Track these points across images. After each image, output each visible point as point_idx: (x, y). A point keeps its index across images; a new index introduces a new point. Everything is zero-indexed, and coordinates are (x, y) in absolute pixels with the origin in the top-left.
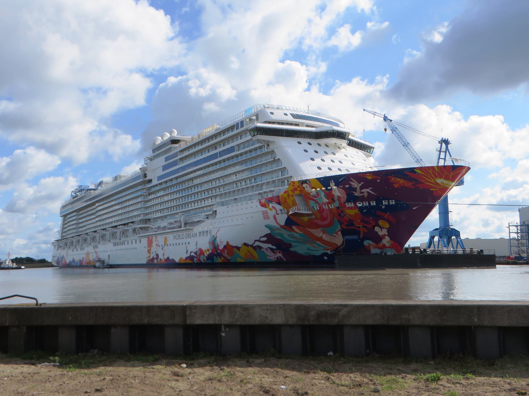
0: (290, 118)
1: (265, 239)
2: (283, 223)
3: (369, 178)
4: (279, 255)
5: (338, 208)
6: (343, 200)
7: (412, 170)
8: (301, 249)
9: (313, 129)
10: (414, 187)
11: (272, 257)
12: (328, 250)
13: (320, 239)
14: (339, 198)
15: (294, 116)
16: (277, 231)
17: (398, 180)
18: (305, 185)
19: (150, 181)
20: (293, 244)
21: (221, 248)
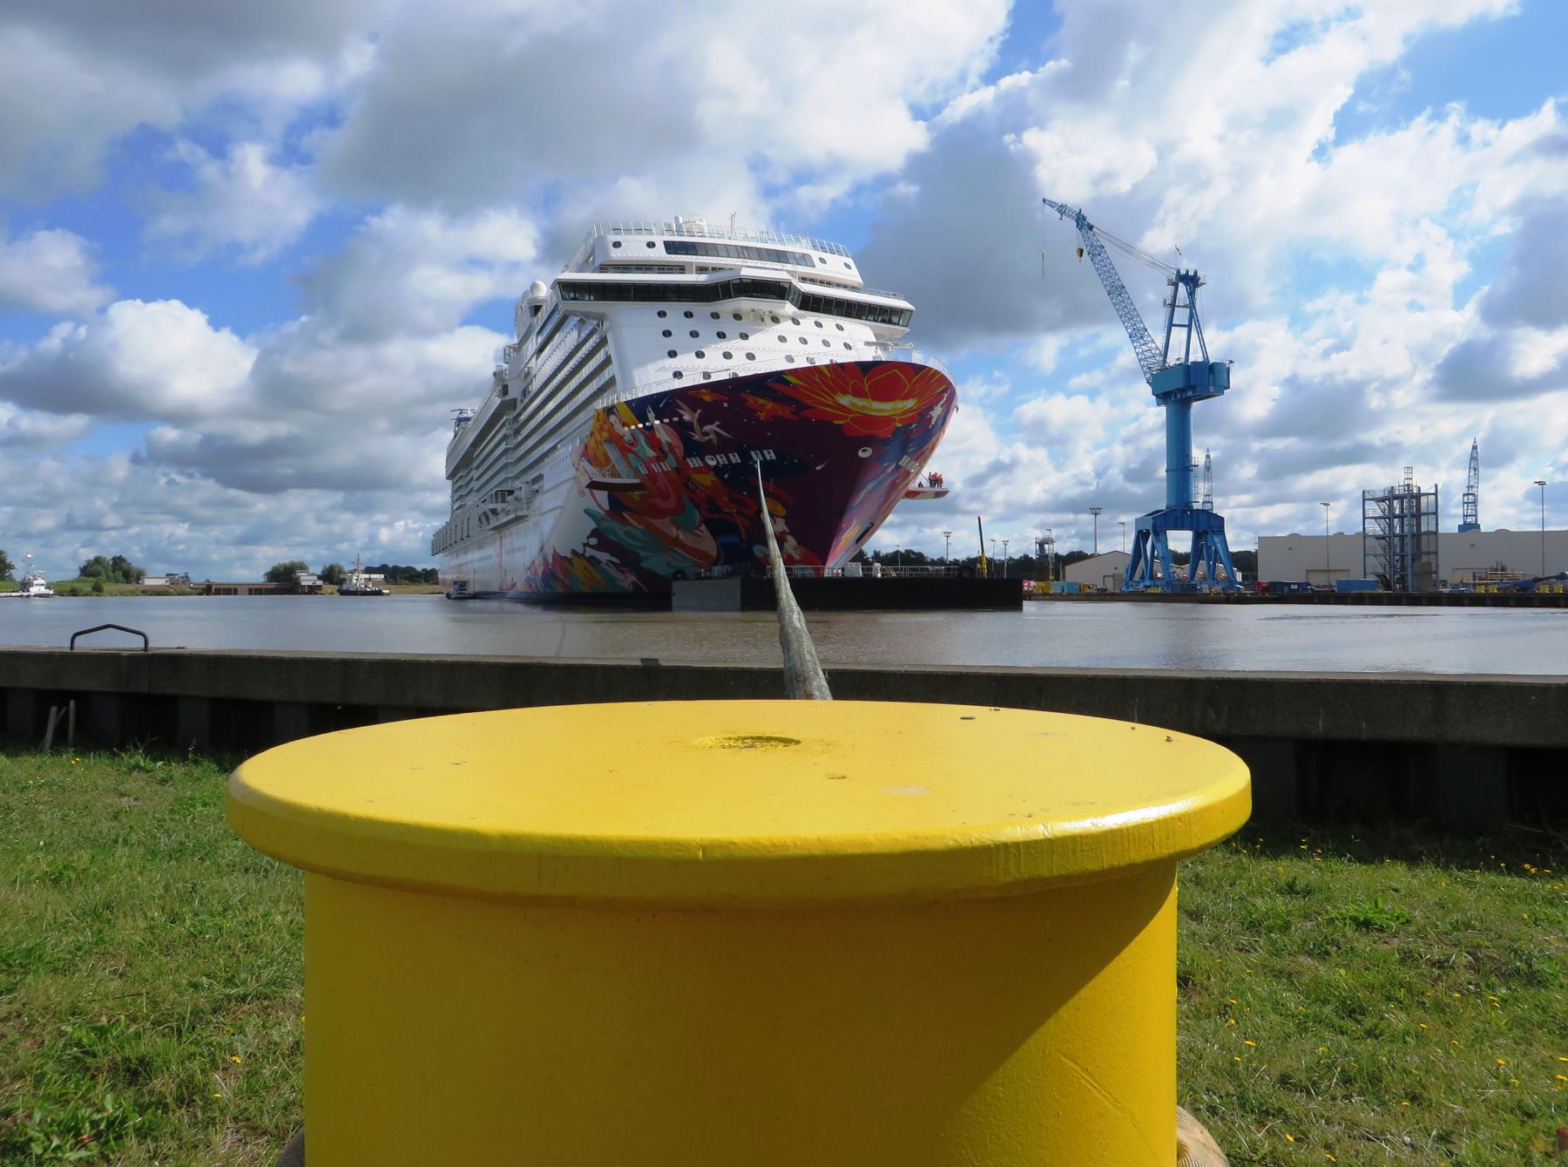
0: (659, 254)
3: (708, 398)
4: (632, 578)
5: (677, 470)
6: (680, 451)
7: (778, 376)
8: (658, 563)
9: (702, 278)
11: (627, 581)
12: (701, 566)
14: (670, 444)
15: (671, 247)
16: (605, 524)
17: (761, 401)
18: (613, 419)
19: (512, 404)
20: (642, 554)
21: (550, 560)
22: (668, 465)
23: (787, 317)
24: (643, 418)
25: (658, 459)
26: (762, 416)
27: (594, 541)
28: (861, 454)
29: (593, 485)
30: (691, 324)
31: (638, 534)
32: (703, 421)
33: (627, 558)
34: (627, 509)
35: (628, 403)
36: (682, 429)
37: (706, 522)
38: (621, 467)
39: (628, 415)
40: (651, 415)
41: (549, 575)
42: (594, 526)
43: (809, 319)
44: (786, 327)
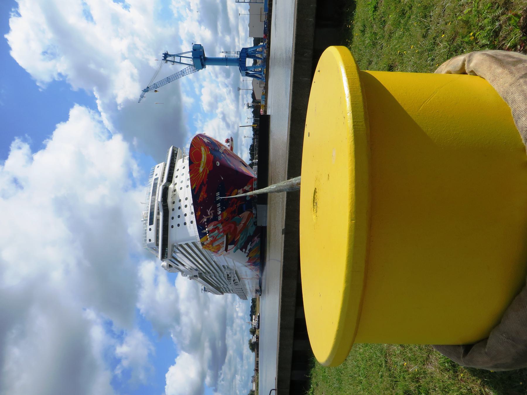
0: (153, 227)
1: (244, 250)
2: (233, 246)
3: (199, 213)
4: (256, 238)
5: (222, 223)
6: (216, 222)
7: (193, 191)
8: (251, 230)
9: (161, 214)
10: (206, 185)
11: (257, 240)
12: (253, 217)
13: (244, 224)
15: (151, 223)
16: (239, 246)
17: (201, 196)
18: (205, 243)
19: (200, 274)
20: (248, 235)
22: (220, 226)
23: (174, 187)
24: (205, 234)
25: (218, 229)
26: (205, 196)
27: (244, 250)
28: (218, 165)
29: (226, 250)
30: (176, 218)
31: (242, 236)
32: (207, 215)
33: (250, 239)
34: (234, 239)
35: (200, 238)
36: (209, 222)
37: (239, 214)
38: (220, 241)
39: (204, 239)
40: (204, 231)
41: (254, 264)
42: (239, 250)
43: (175, 180)
44: (177, 187)
